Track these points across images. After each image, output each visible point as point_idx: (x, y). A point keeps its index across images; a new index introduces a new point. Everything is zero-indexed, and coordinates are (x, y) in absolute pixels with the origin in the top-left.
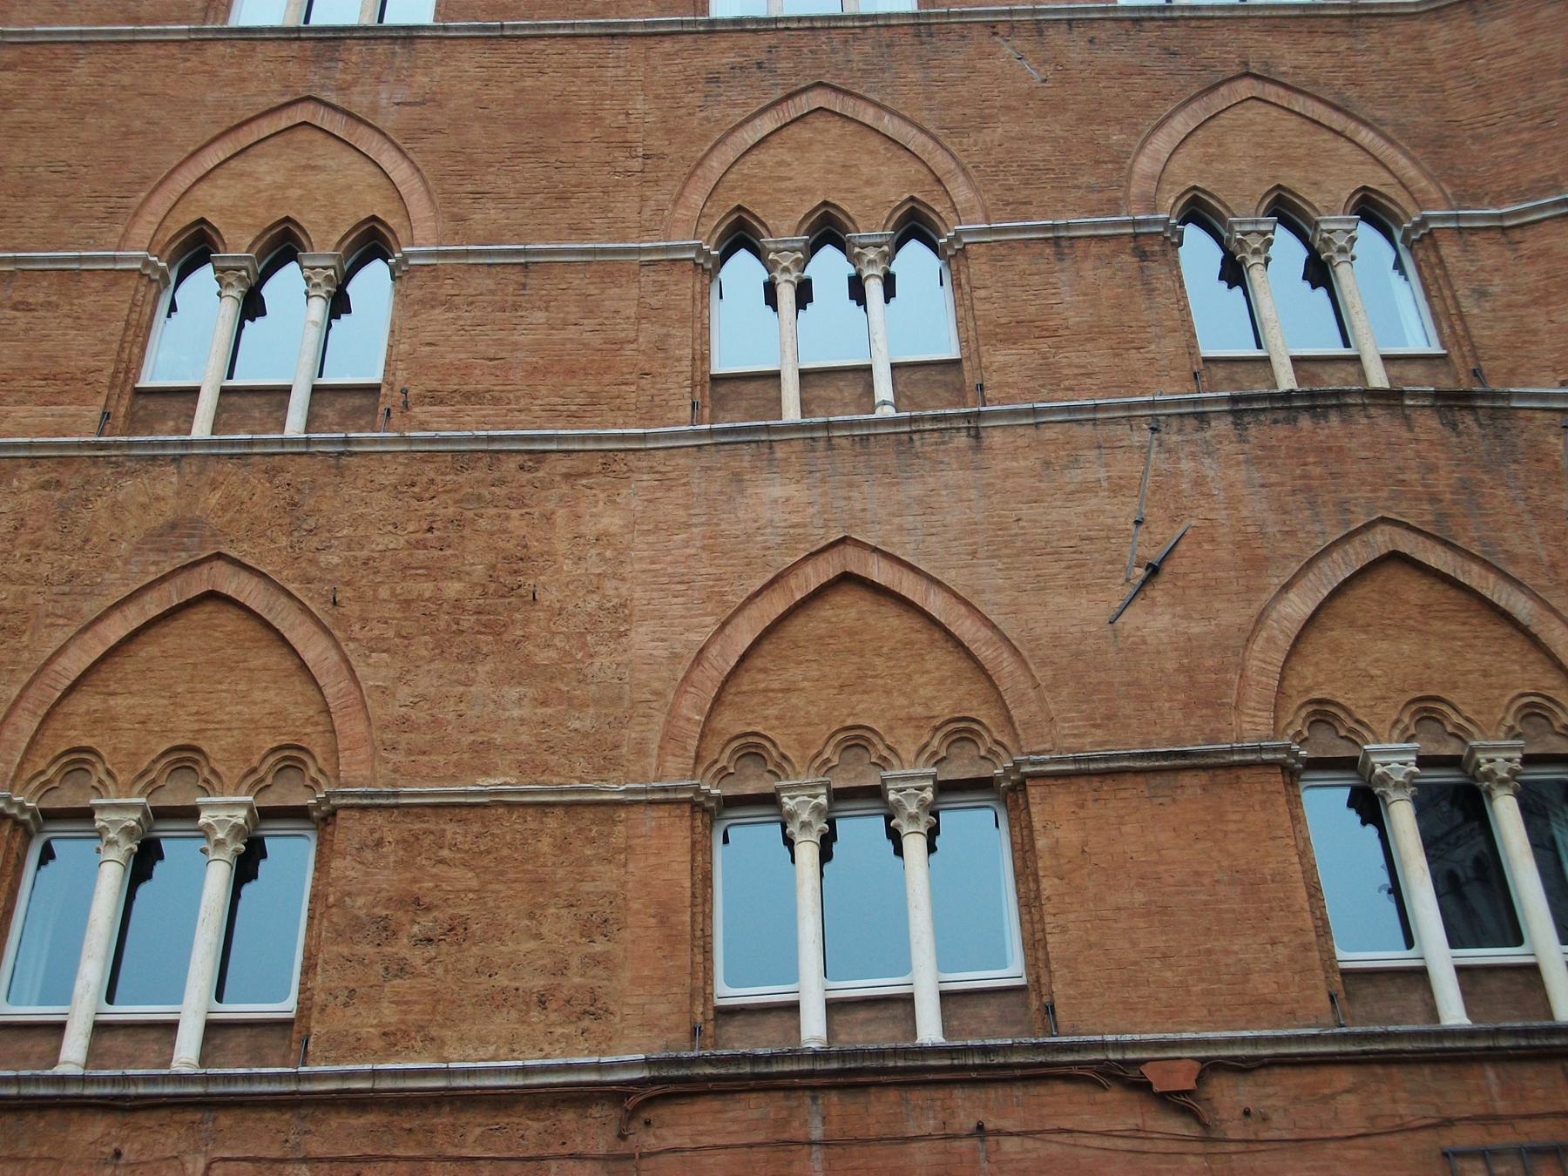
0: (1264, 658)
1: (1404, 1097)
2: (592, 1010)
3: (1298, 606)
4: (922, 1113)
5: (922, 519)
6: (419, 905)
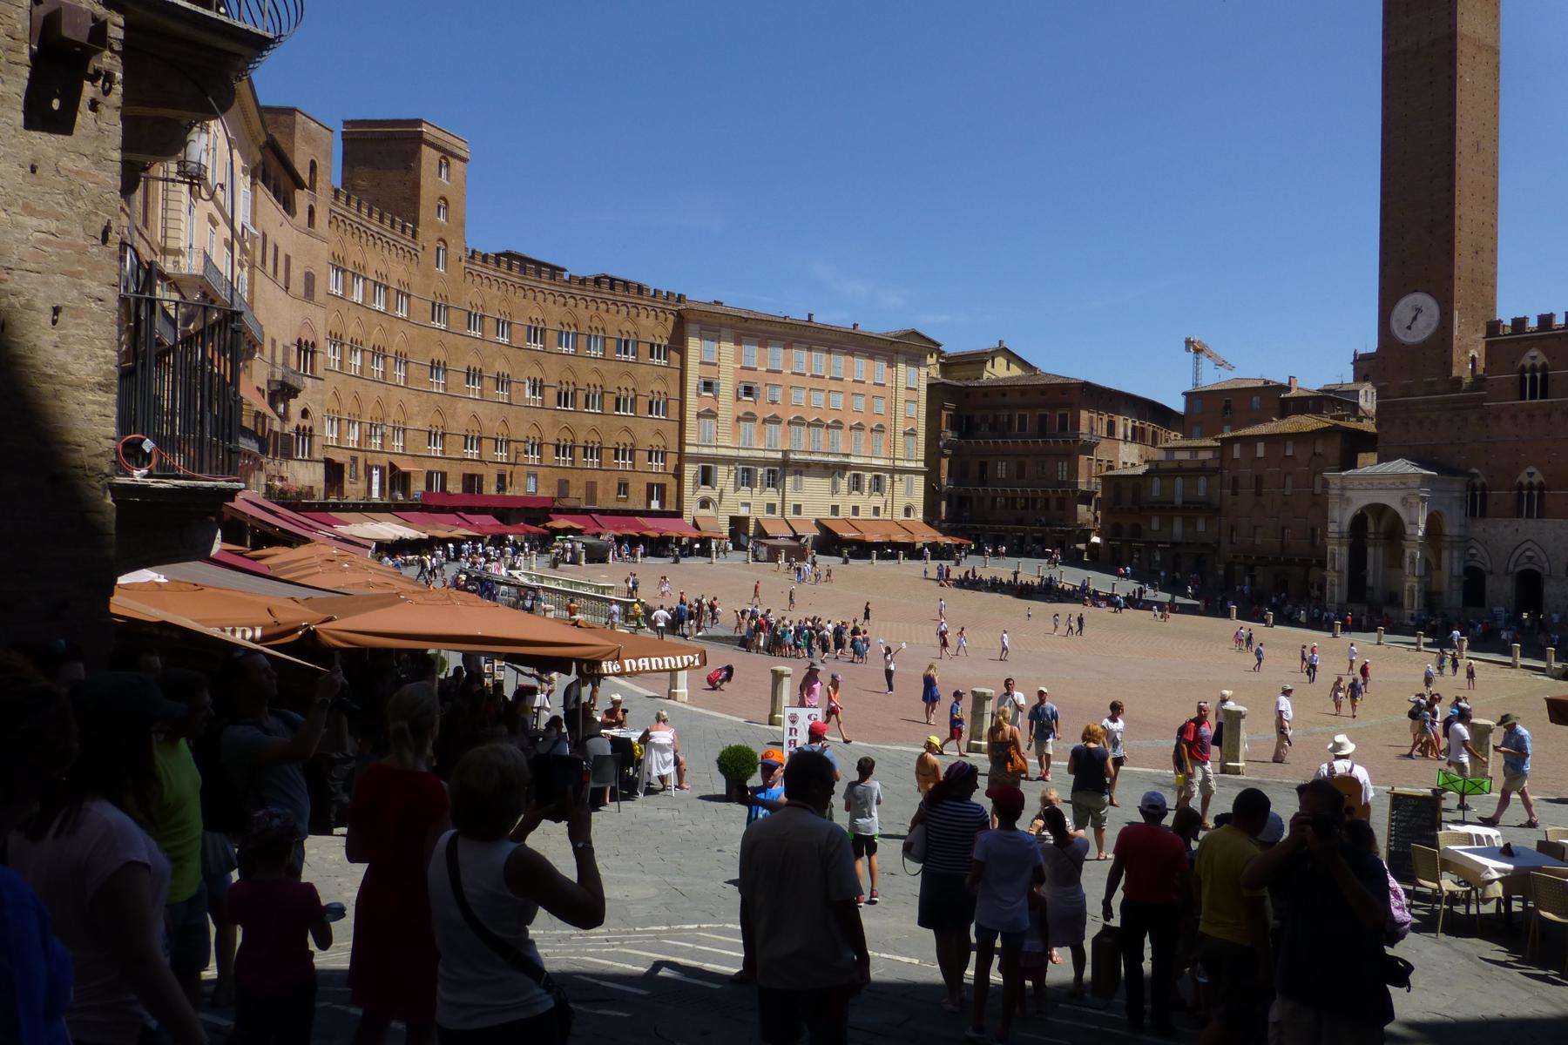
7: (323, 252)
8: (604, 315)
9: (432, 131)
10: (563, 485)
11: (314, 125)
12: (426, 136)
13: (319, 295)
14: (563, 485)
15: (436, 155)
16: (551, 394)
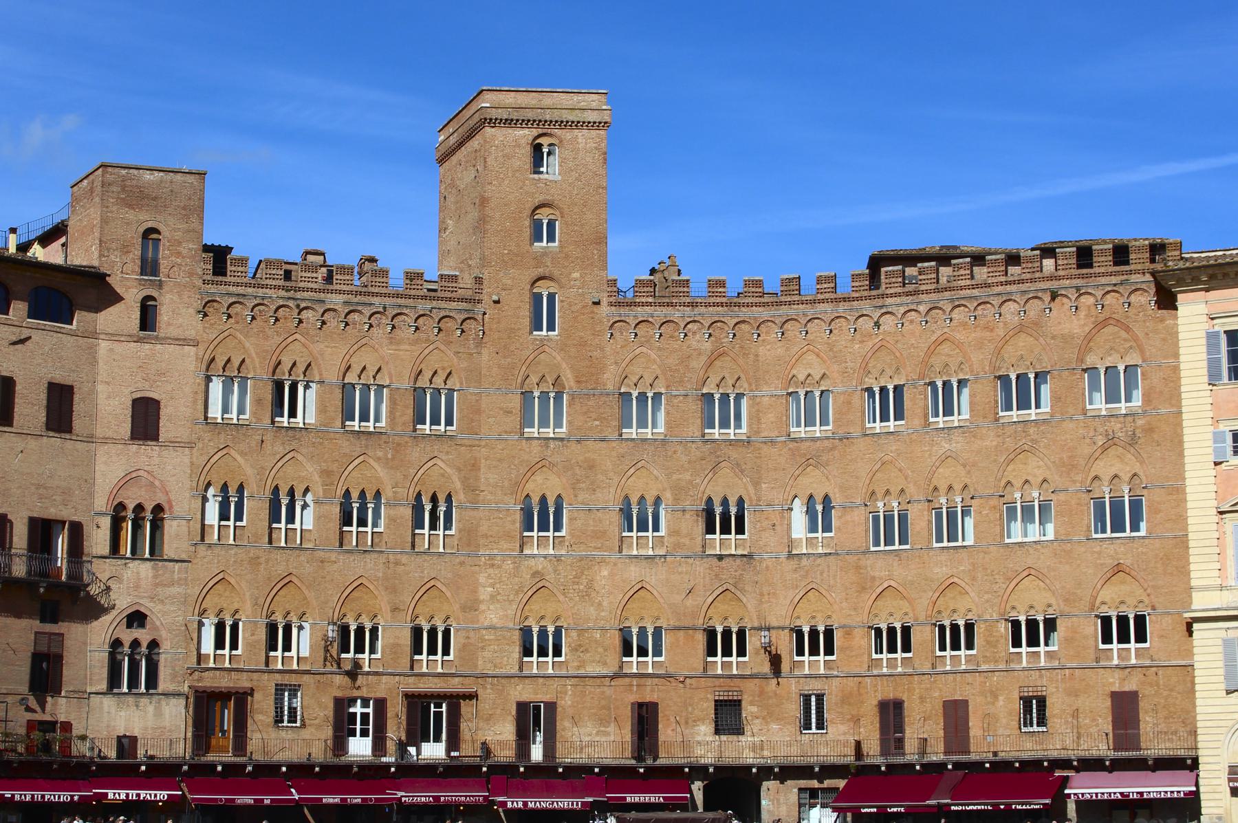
0: (704, 609)
1: (710, 682)
2: (605, 664)
3: (710, 599)
4: (649, 681)
5: (654, 577)
6: (580, 646)
7: (188, 361)
8: (960, 336)
9: (510, 99)
10: (892, 714)
11: (148, 176)
12: (494, 114)
13: (166, 429)
14: (892, 714)
15: (525, 135)
16: (852, 525)
